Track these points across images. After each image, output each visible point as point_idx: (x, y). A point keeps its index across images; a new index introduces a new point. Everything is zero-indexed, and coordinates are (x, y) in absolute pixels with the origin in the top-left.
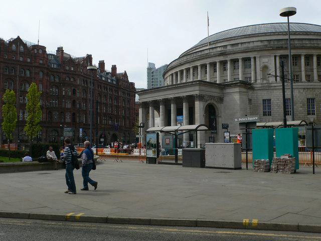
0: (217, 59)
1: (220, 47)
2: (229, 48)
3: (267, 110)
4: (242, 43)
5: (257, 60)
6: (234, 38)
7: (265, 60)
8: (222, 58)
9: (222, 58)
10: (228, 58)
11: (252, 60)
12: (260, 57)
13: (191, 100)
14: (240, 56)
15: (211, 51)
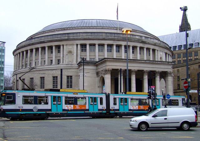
0: (139, 45)
1: (138, 36)
2: (143, 38)
3: (69, 84)
4: (150, 38)
5: (159, 52)
6: (146, 33)
7: (161, 53)
8: (142, 45)
9: (142, 45)
10: (146, 46)
11: (156, 51)
12: (160, 51)
13: (164, 75)
14: (152, 47)
15: (132, 36)
